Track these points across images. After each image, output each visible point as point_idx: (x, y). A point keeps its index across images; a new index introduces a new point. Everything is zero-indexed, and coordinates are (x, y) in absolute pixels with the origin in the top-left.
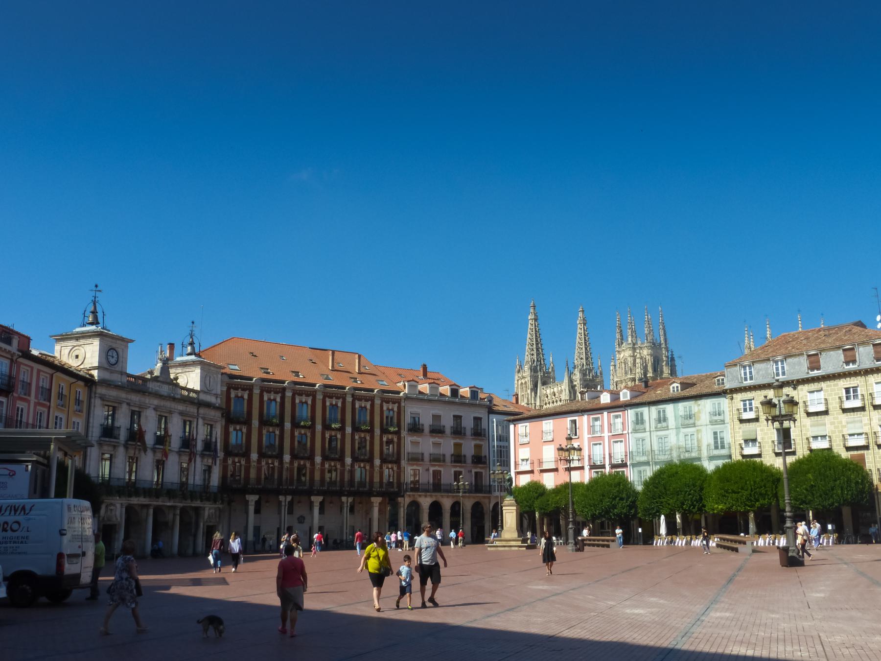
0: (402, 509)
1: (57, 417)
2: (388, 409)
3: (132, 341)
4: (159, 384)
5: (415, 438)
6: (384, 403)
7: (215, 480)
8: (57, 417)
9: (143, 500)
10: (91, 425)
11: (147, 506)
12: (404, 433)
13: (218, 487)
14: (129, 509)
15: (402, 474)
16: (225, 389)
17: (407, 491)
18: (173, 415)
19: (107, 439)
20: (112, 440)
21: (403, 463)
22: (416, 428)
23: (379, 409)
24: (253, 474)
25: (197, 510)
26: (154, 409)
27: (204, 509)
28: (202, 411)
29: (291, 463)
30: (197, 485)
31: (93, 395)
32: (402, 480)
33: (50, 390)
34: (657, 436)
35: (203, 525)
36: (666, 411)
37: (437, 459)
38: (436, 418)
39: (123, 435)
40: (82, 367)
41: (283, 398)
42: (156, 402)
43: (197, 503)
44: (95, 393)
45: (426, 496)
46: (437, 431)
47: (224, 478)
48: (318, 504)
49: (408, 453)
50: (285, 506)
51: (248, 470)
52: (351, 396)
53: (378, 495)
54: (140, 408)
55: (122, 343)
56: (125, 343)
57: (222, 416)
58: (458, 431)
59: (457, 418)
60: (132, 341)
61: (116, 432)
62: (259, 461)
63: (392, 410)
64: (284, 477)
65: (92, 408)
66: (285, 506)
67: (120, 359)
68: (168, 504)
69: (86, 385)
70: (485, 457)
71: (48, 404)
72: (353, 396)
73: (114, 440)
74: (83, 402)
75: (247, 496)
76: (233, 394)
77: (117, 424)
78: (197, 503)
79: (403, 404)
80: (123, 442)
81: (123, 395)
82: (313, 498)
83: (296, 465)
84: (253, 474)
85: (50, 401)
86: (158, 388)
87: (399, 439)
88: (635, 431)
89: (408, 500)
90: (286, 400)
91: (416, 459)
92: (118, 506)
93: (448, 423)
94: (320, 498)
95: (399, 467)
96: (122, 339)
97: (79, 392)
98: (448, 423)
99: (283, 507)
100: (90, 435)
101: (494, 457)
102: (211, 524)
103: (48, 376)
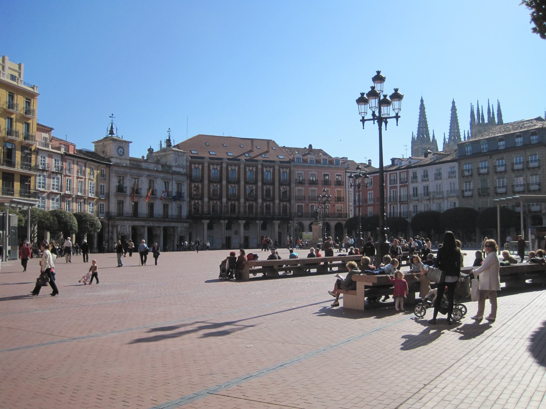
3: (131, 142)
4: (148, 163)
6: (281, 168)
7: (185, 213)
9: (142, 223)
11: (143, 227)
13: (187, 216)
14: (134, 228)
16: (188, 164)
17: (294, 217)
18: (157, 179)
19: (120, 193)
20: (122, 193)
24: (206, 209)
25: (173, 227)
26: (146, 177)
27: (177, 227)
28: (174, 176)
29: (227, 202)
30: (174, 215)
31: (111, 171)
35: (178, 236)
39: (129, 191)
41: (221, 168)
42: (147, 173)
43: (173, 224)
44: (112, 170)
45: (307, 220)
47: (190, 211)
49: (296, 196)
51: (203, 206)
52: (261, 165)
53: (278, 219)
54: (138, 177)
56: (127, 144)
57: (187, 179)
60: (131, 142)
61: (124, 189)
62: (209, 202)
64: (223, 211)
65: (111, 178)
66: (224, 225)
68: (156, 225)
72: (262, 165)
74: (105, 175)
75: (203, 221)
76: (193, 166)
77: (125, 185)
78: (173, 224)
79: (292, 169)
80: (129, 195)
81: (128, 171)
83: (230, 204)
84: (206, 209)
86: (148, 166)
90: (223, 169)
92: (127, 227)
94: (244, 222)
95: (290, 204)
96: (126, 142)
97: (103, 170)
102: (182, 235)
103: (83, 164)
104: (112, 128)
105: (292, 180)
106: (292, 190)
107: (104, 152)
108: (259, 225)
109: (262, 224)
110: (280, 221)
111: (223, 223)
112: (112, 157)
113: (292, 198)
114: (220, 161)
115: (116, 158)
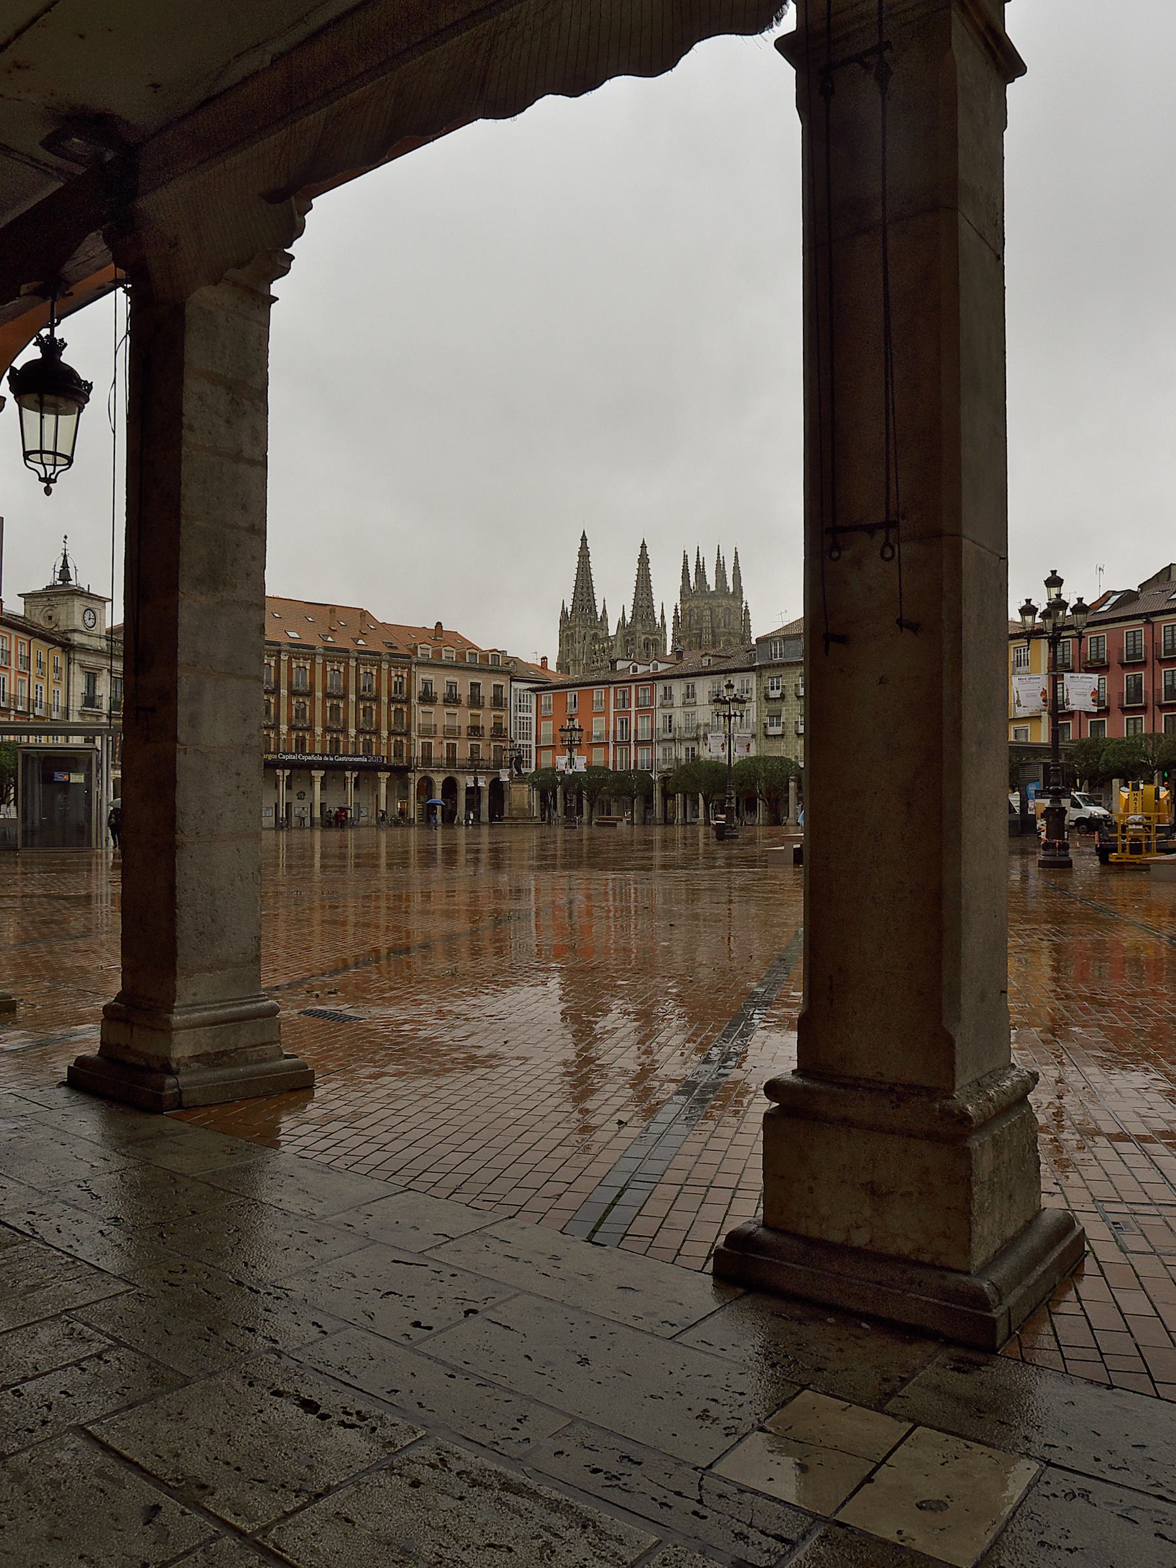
0: (412, 785)
1: (37, 686)
2: (397, 675)
5: (427, 708)
8: (37, 686)
10: (71, 693)
12: (414, 701)
15: (412, 747)
19: (89, 709)
21: (414, 734)
22: (427, 698)
23: (387, 675)
32: (413, 756)
33: (29, 658)
34: (684, 712)
36: (695, 686)
37: (451, 732)
38: (452, 686)
40: (56, 629)
46: (452, 700)
48: (320, 779)
49: (419, 725)
50: (283, 781)
55: (99, 603)
56: (102, 604)
58: (475, 701)
59: (475, 686)
61: (97, 701)
63: (402, 676)
66: (283, 781)
67: (98, 620)
69: (63, 651)
70: (506, 729)
71: (28, 672)
73: (97, 710)
77: (98, 693)
79: (413, 670)
82: (314, 773)
83: (294, 736)
85: (30, 670)
87: (409, 709)
88: (663, 706)
89: (419, 776)
91: (427, 732)
93: (464, 692)
94: (322, 773)
95: (409, 739)
98: (464, 692)
99: (281, 782)
100: (71, 704)
101: (516, 729)
103: (26, 642)
104: (65, 565)
105: (413, 692)
106: (413, 711)
107: (50, 618)
108: (349, 781)
109: (355, 778)
110: (389, 774)
111: (281, 774)
112: (74, 631)
113: (413, 729)
114: (276, 648)
115: (81, 632)
